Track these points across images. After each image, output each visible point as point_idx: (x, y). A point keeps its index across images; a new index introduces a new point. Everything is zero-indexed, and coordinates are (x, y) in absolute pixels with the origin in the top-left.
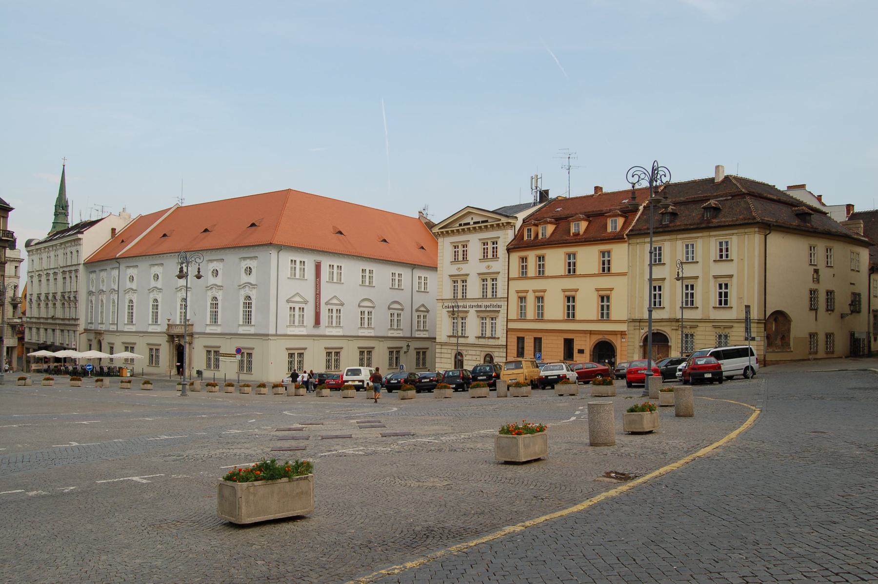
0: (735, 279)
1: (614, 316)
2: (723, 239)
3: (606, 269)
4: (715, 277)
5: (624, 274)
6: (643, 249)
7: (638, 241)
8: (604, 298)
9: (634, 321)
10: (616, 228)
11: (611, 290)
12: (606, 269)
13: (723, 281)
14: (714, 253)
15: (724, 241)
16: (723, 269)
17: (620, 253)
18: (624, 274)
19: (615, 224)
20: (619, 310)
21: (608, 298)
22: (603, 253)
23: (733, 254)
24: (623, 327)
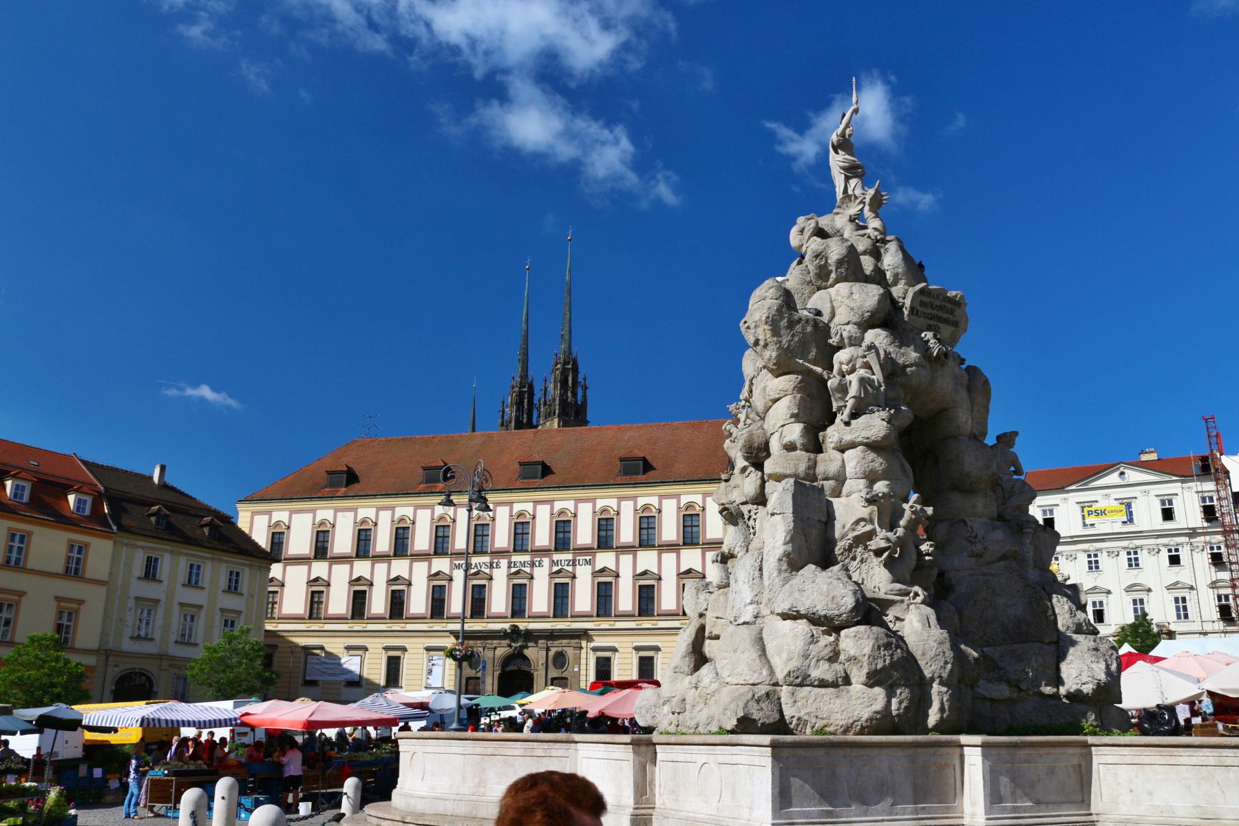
3: (74, 570)
4: (223, 610)
12: (74, 570)
13: (230, 616)
15: (235, 570)
17: (101, 552)
20: (87, 634)
24: (91, 660)
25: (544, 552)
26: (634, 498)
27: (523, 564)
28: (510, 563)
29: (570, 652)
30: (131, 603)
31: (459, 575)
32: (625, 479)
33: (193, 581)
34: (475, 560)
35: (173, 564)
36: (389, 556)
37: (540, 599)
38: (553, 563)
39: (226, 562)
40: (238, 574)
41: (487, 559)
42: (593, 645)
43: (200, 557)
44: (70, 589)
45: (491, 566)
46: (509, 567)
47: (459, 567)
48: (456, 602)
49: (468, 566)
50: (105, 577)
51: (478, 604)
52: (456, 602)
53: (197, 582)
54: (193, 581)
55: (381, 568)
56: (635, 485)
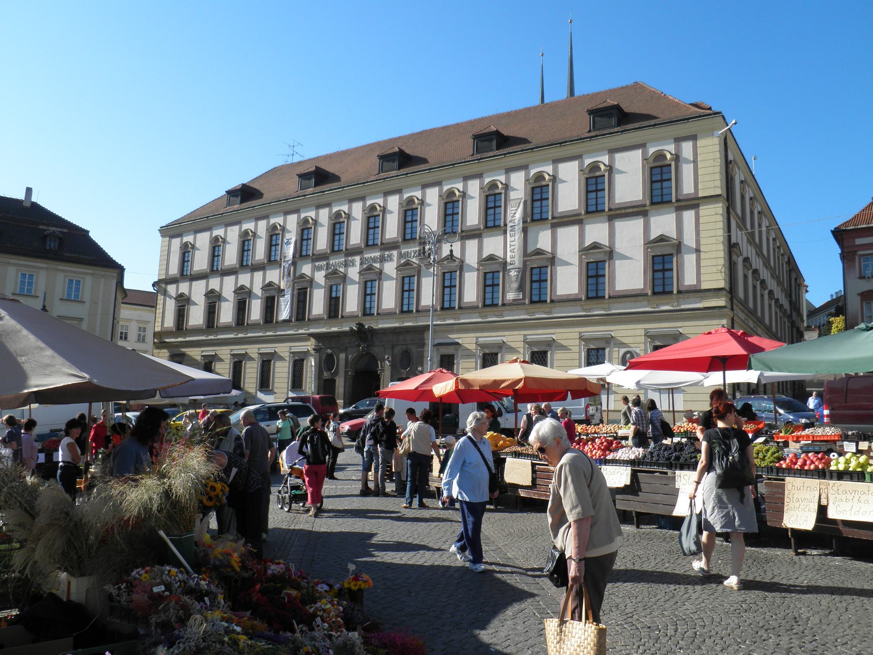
25: (392, 246)
27: (374, 260)
29: (414, 350)
31: (320, 277)
32: (479, 156)
37: (389, 298)
38: (401, 256)
39: (63, 271)
40: (78, 282)
42: (437, 342)
46: (361, 264)
47: (319, 269)
48: (318, 305)
51: (334, 305)
52: (318, 305)
55: (258, 275)
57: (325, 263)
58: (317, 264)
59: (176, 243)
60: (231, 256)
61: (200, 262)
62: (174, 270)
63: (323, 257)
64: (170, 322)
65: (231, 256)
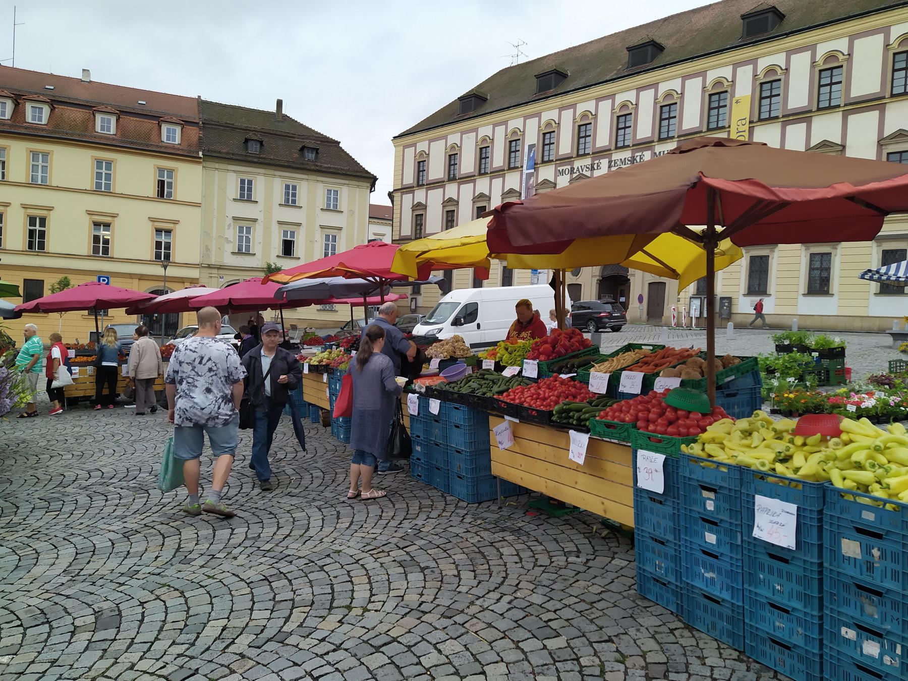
0: (344, 233)
1: (178, 255)
2: (333, 188)
4: (322, 227)
5: (197, 205)
6: (229, 179)
7: (217, 166)
8: (163, 231)
9: (209, 267)
10: (40, 119)
11: (50, 209)
13: (331, 232)
14: (321, 202)
15: (333, 189)
16: (290, 215)
17: (189, 178)
18: (197, 205)
19: (171, 135)
20: (185, 249)
21: (43, 222)
22: (161, 170)
23: (343, 205)
26: (754, 61)
28: (610, 162)
30: (230, 221)
33: (290, 201)
34: (578, 164)
35: (269, 186)
36: (503, 170)
41: (587, 161)
43: (294, 178)
44: (163, 210)
45: (593, 169)
46: (610, 167)
47: (562, 173)
49: (572, 169)
50: (198, 200)
53: (294, 201)
54: (290, 201)
55: (497, 182)
56: (755, 43)
57: (569, 167)
58: (560, 169)
59: (410, 152)
60: (468, 164)
61: (436, 170)
62: (409, 179)
63: (567, 159)
64: (407, 231)
65: (468, 164)
